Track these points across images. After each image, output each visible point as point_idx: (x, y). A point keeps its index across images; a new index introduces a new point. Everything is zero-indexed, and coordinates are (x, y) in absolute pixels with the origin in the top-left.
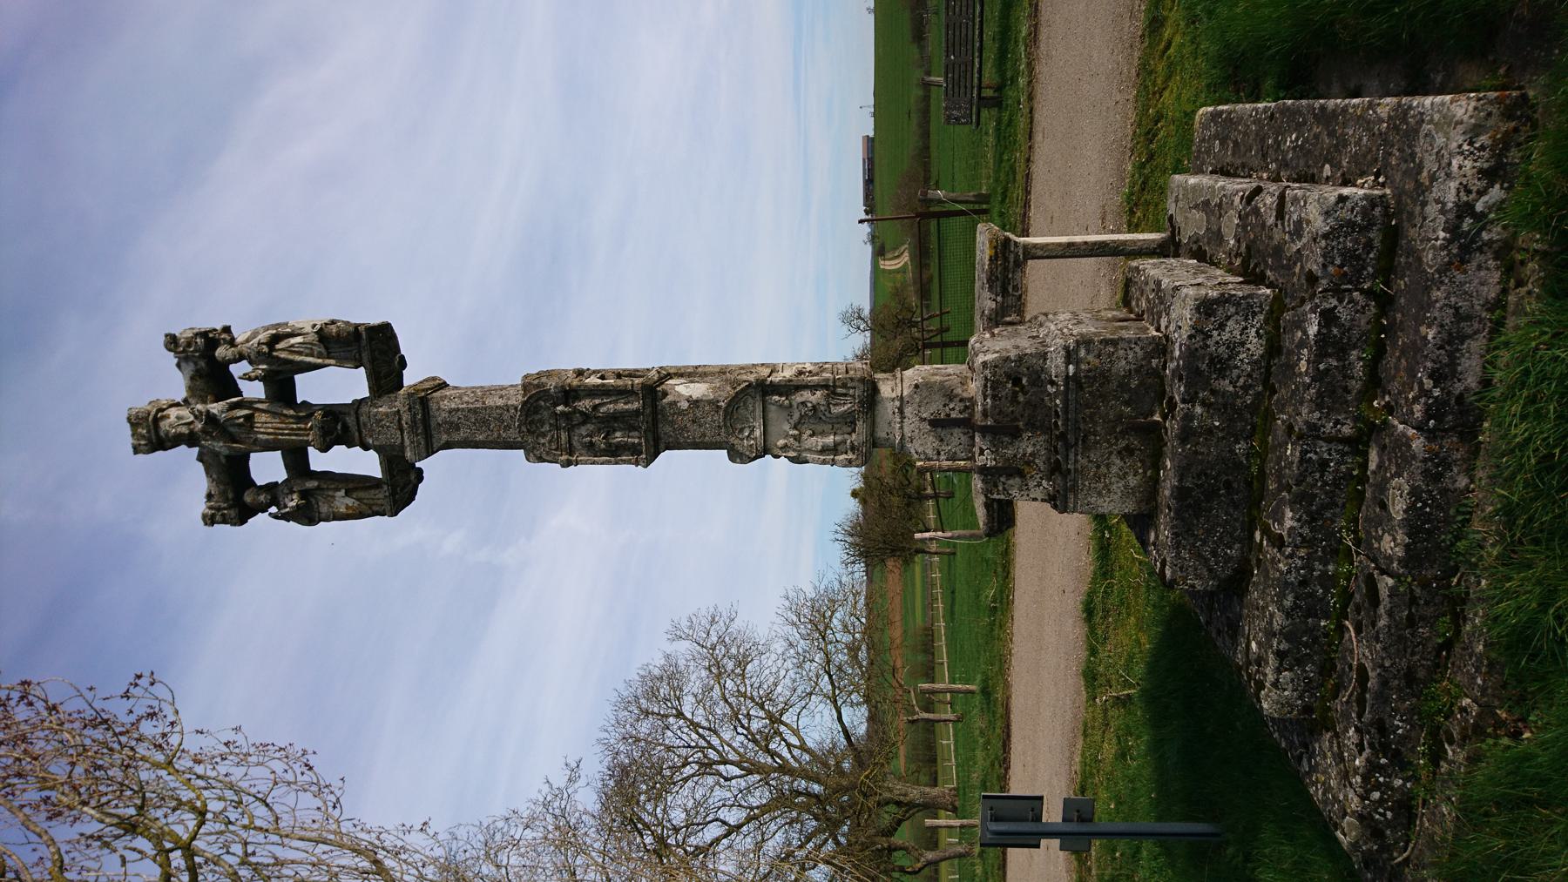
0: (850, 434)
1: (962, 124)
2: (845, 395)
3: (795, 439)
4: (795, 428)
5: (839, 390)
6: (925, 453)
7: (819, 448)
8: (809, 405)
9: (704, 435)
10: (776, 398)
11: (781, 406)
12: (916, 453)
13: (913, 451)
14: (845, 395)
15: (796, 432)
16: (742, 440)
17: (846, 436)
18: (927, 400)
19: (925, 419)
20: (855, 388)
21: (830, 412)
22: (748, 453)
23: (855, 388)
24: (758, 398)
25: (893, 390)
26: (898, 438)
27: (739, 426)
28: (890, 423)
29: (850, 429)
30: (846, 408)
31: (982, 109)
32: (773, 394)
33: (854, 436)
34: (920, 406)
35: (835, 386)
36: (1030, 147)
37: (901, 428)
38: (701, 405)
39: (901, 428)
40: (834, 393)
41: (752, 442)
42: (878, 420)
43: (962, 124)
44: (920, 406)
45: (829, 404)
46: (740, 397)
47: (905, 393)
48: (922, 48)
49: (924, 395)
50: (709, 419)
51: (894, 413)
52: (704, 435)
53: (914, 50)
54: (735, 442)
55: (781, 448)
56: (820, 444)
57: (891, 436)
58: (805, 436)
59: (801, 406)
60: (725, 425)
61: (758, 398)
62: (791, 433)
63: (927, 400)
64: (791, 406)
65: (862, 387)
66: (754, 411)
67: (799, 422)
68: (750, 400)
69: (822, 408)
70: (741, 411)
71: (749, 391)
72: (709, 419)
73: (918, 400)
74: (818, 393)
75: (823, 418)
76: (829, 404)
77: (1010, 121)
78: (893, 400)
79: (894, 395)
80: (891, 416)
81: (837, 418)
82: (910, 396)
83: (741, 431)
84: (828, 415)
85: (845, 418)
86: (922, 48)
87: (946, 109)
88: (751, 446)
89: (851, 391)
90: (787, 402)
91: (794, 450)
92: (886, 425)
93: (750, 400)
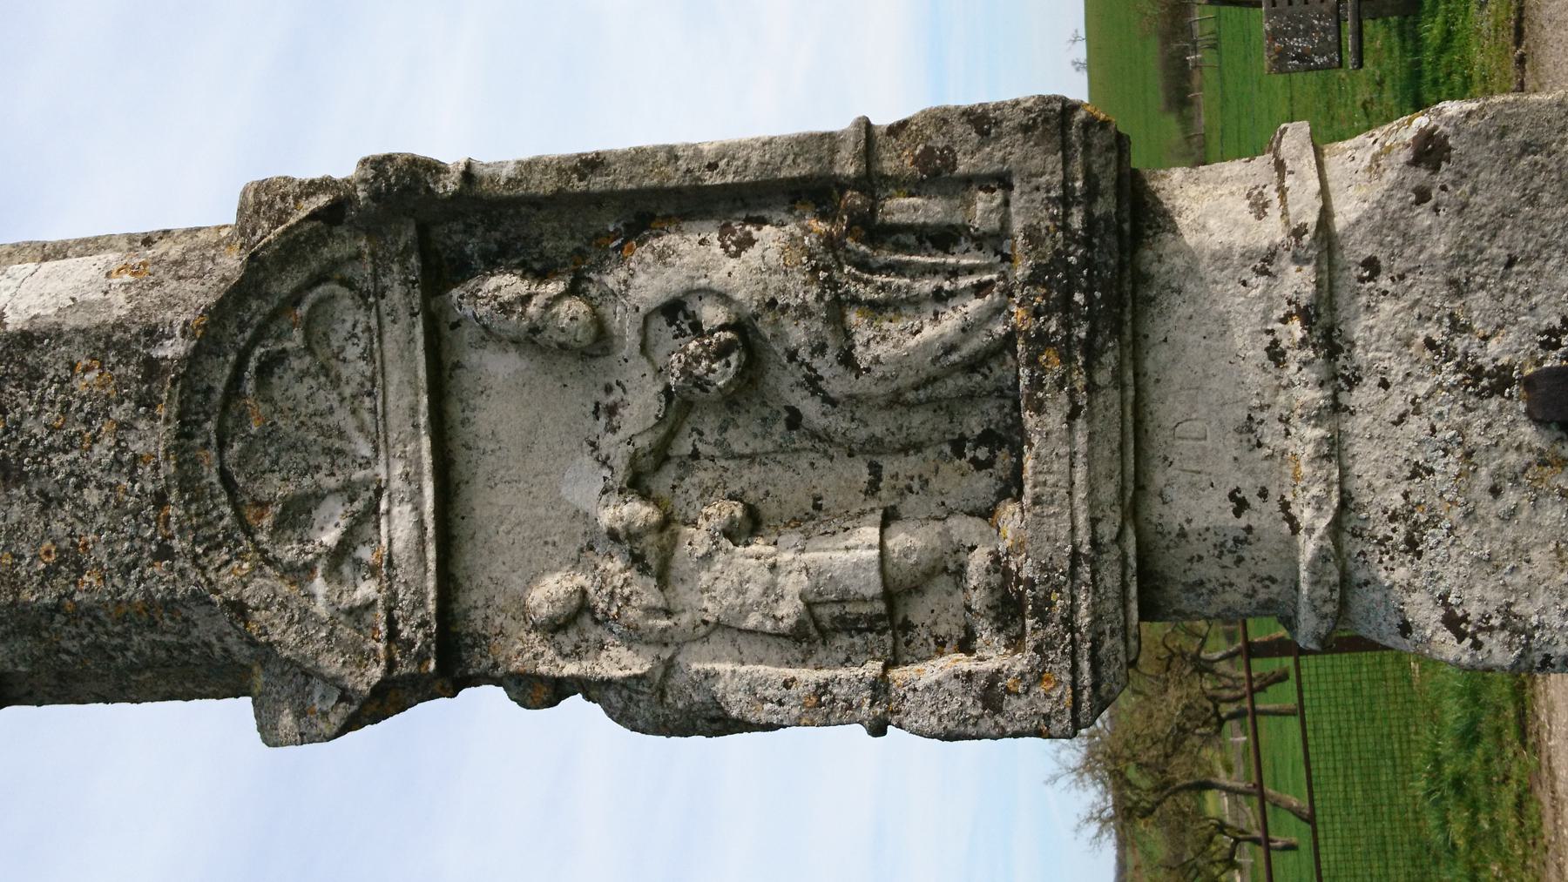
0: (987, 514)
1: (1317, 68)
2: (943, 237)
3: (637, 560)
4: (636, 484)
5: (902, 208)
6: (1511, 622)
7: (789, 610)
8: (712, 315)
9: (72, 560)
10: (508, 284)
11: (532, 340)
12: (1453, 622)
13: (1425, 614)
14: (943, 237)
15: (638, 512)
16: (300, 573)
17: (964, 528)
18: (1514, 238)
19: (1502, 380)
20: (1003, 181)
21: (847, 359)
22: (332, 664)
23: (1003, 181)
24: (396, 295)
25: (1260, 208)
26: (1314, 520)
27: (277, 487)
28: (1249, 426)
29: (983, 485)
30: (950, 322)
31: (1369, 25)
32: (492, 264)
33: (1011, 517)
34: (1458, 288)
35: (872, 182)
36: (1521, 61)
37: (1334, 450)
38: (53, 362)
39: (1334, 450)
40: (878, 233)
41: (367, 589)
42: (1168, 409)
43: (1317, 68)
44: (1458, 288)
45: (837, 308)
46: (285, 286)
47: (1346, 212)
48: (1186, 122)
49: (1485, 204)
50: (102, 451)
51: (1276, 354)
52: (72, 560)
53: (1171, 123)
54: (260, 588)
55: (555, 627)
56: (793, 583)
57: (1263, 517)
58: (696, 539)
59: (662, 330)
60: (188, 483)
61: (396, 295)
62: (607, 517)
63: (1514, 238)
64: (601, 339)
65: (1048, 167)
66: (373, 386)
67: (661, 455)
68: (349, 315)
69: (797, 334)
70: (293, 387)
71: (339, 248)
72: (102, 451)
73: (1440, 246)
74: (770, 239)
75: (811, 408)
76: (837, 308)
77: (1448, 36)
78: (1266, 263)
79: (1272, 230)
80: (1255, 376)
81: (895, 401)
82: (1386, 223)
83: (296, 514)
84: (838, 383)
85: (945, 407)
86: (1186, 122)
87: (1274, 35)
88: (357, 613)
89: (982, 209)
90: (573, 308)
91: (634, 637)
92: (1231, 446)
93: (349, 315)
